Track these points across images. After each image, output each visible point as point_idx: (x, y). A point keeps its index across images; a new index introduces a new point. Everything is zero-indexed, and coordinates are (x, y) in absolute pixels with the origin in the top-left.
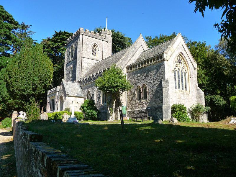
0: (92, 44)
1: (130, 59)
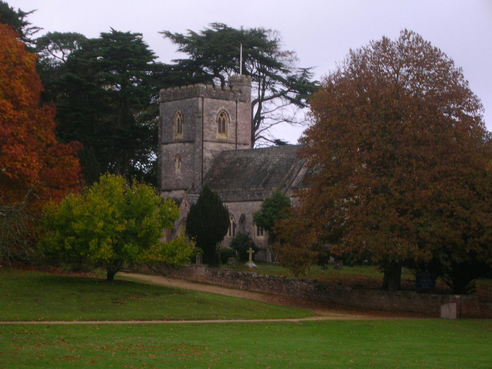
0: (218, 111)
1: (296, 176)
